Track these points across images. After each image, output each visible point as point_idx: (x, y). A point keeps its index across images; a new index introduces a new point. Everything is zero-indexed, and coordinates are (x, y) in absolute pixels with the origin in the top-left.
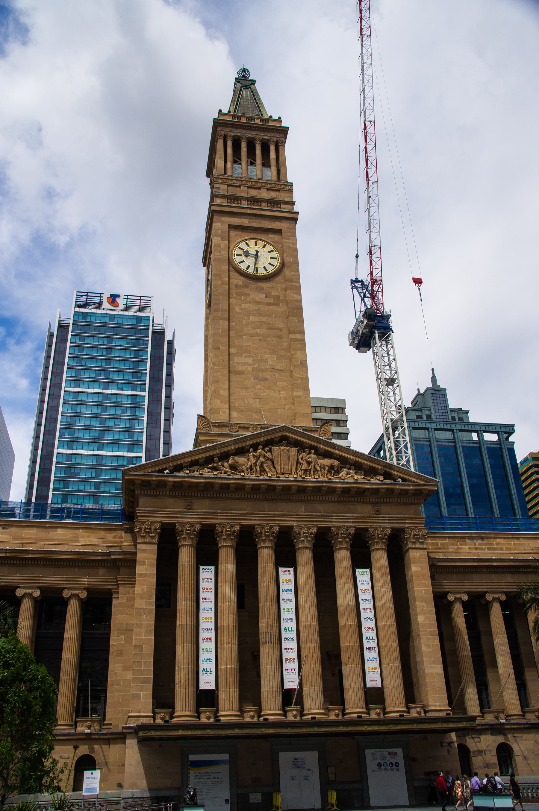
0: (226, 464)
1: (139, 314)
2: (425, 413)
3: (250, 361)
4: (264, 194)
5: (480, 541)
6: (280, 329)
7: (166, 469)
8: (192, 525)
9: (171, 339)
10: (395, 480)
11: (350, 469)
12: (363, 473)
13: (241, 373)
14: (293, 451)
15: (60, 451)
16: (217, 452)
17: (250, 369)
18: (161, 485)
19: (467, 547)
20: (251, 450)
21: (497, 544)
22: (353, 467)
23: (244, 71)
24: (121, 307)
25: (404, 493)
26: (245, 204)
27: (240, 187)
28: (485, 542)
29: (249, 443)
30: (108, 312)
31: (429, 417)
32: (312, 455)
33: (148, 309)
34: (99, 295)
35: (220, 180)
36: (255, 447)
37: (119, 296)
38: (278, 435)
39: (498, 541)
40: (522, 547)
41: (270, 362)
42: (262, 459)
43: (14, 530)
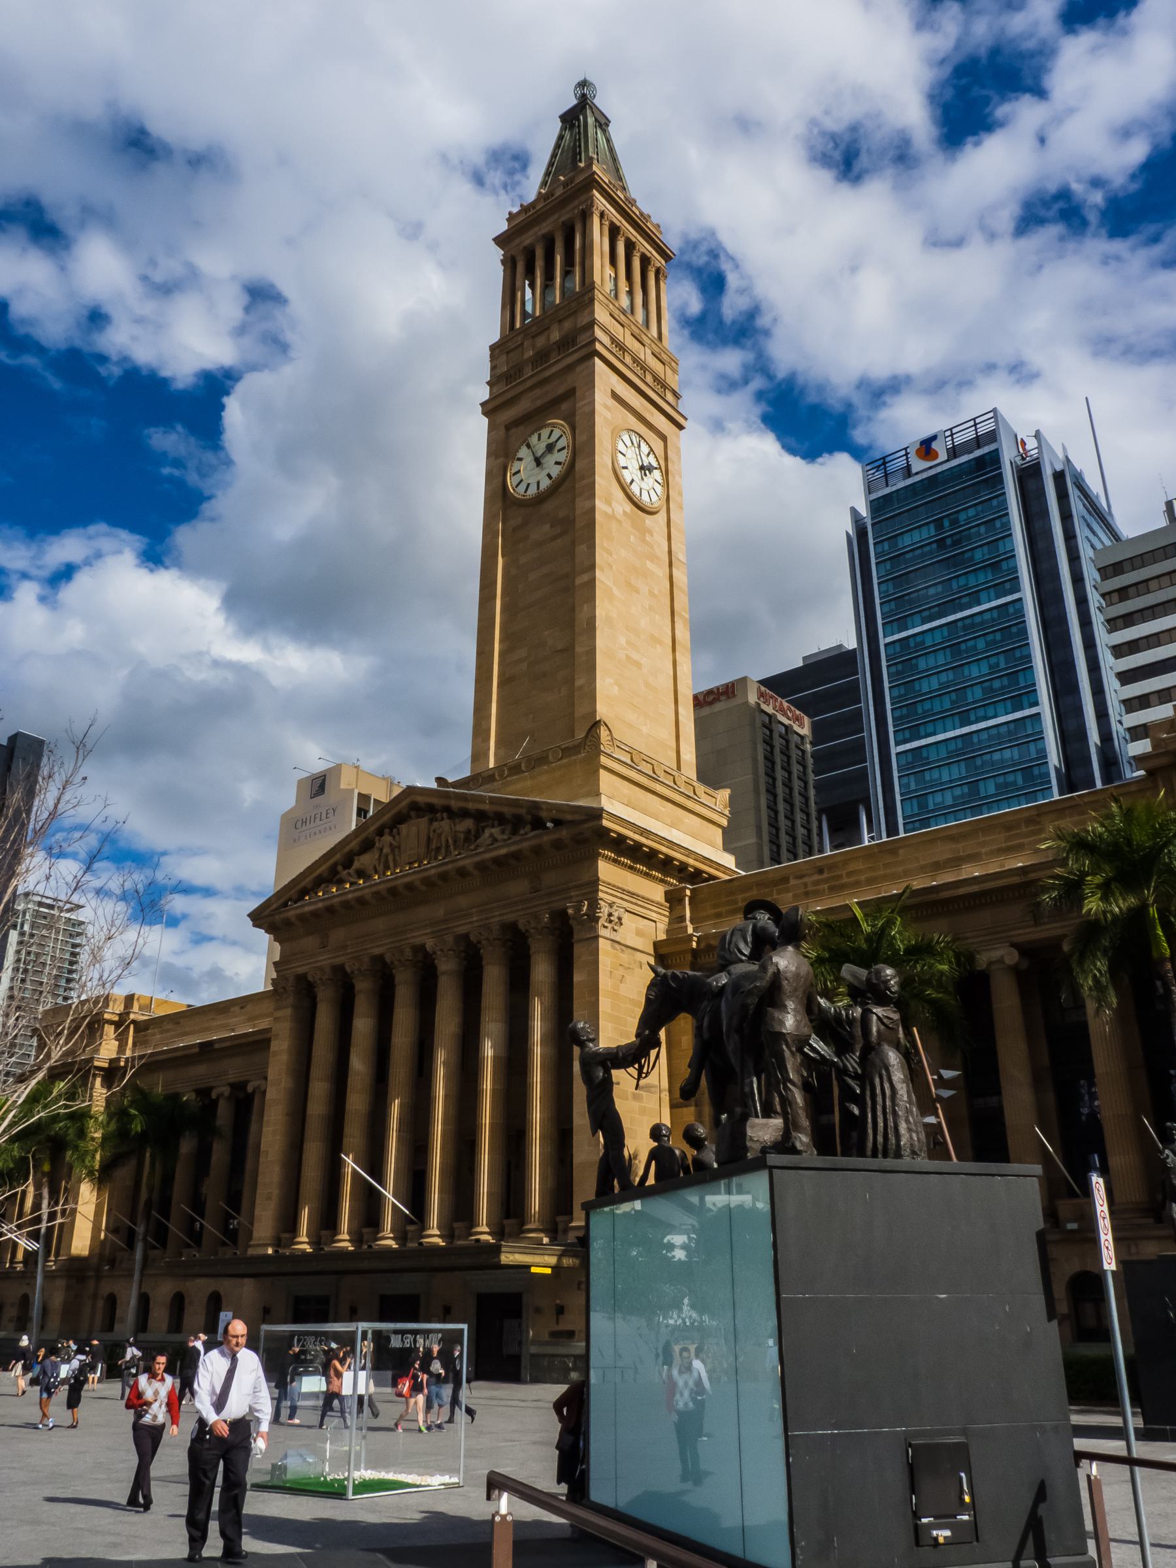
0: (352, 871)
3: (521, 653)
4: (555, 336)
5: (816, 877)
8: (321, 969)
9: (1059, 468)
11: (493, 826)
12: (509, 828)
14: (423, 822)
15: (901, 748)
16: (338, 857)
18: (288, 923)
19: (790, 895)
21: (849, 874)
22: (496, 823)
24: (943, 456)
25: (558, 845)
27: (522, 344)
28: (825, 875)
29: (372, 829)
30: (925, 475)
34: (903, 452)
36: (380, 833)
37: (934, 438)
38: (404, 803)
39: (852, 867)
40: (901, 869)
42: (386, 850)
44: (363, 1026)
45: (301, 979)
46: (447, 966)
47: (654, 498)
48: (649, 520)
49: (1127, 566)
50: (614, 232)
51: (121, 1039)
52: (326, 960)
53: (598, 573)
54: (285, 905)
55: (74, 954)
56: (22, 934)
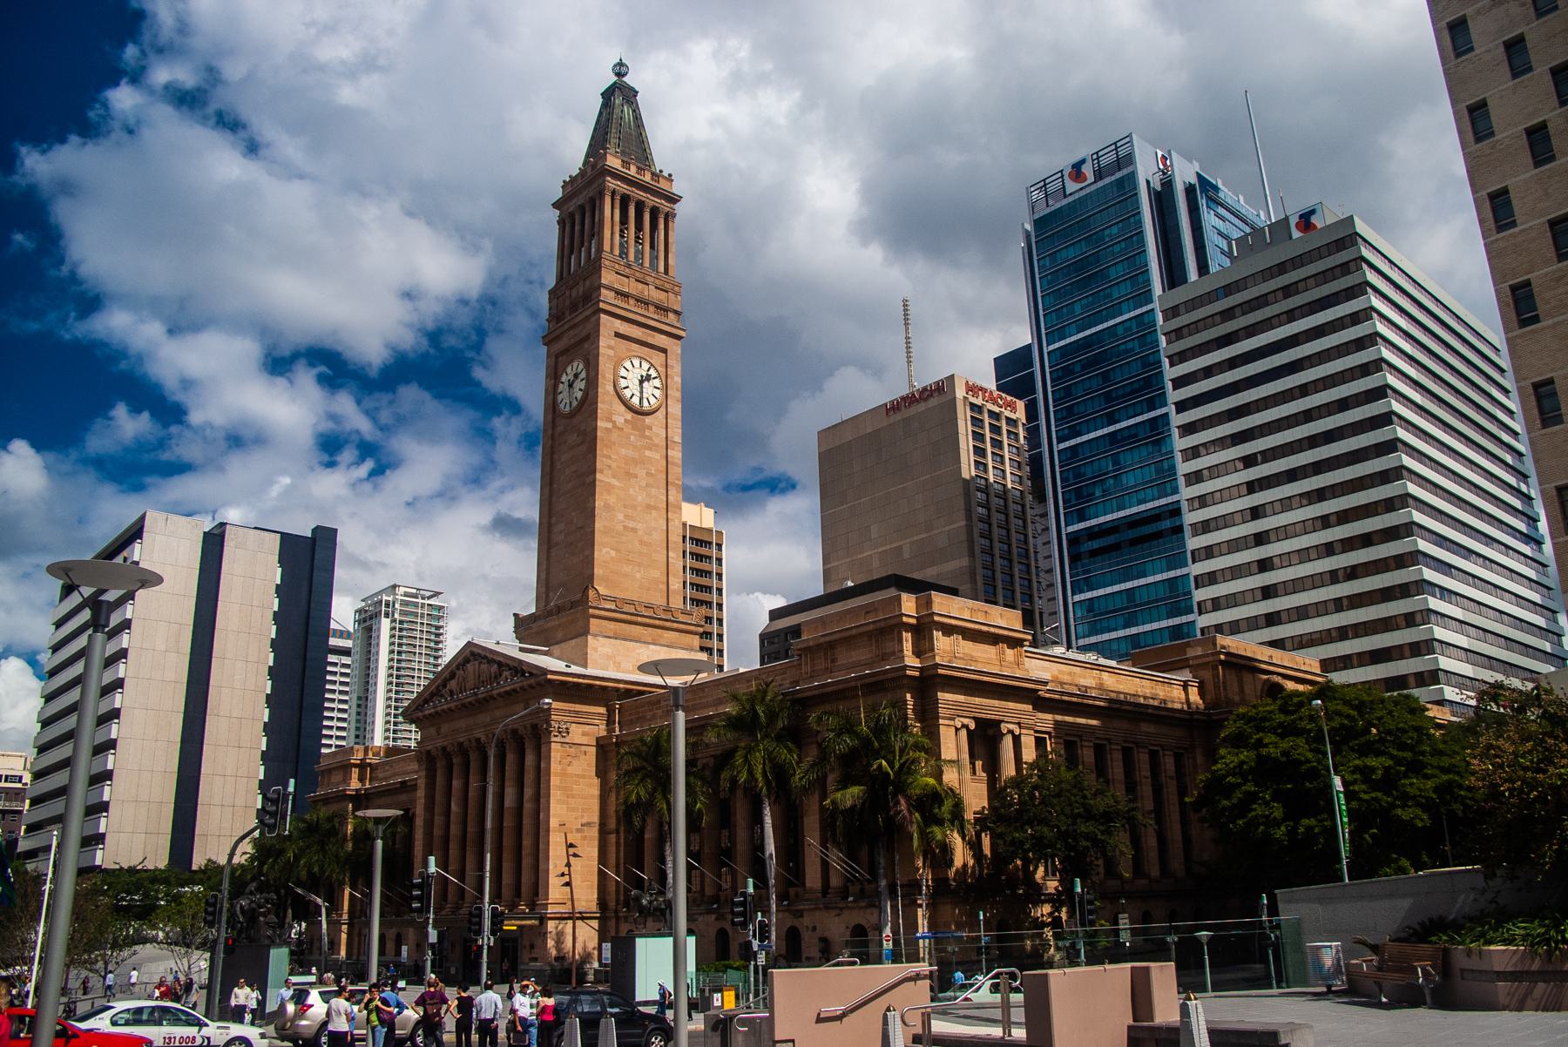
1: (1118, 175)
3: (561, 526)
23: (621, 64)
24: (1091, 179)
30: (1077, 196)
33: (1129, 159)
37: (1083, 161)
44: (457, 784)
45: (428, 752)
46: (492, 753)
47: (653, 401)
48: (648, 420)
49: (1182, 309)
50: (625, 200)
51: (361, 779)
52: (440, 743)
53: (598, 476)
55: (438, 635)
56: (394, 621)
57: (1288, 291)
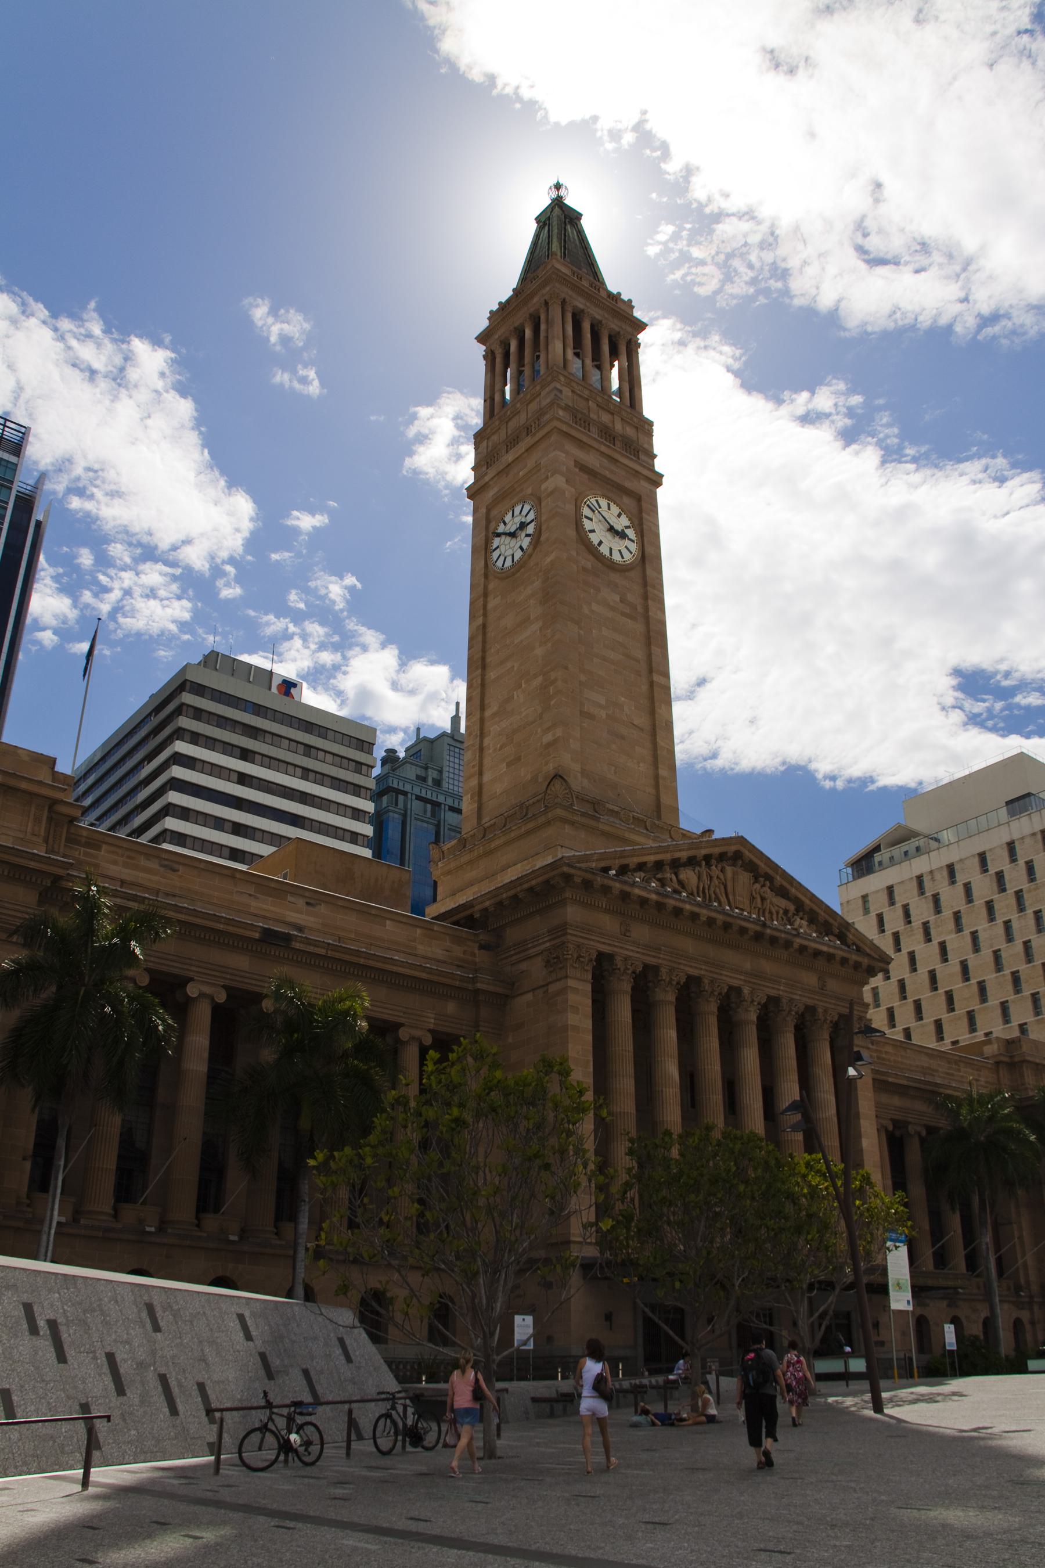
2: (432, 774)
6: (637, 660)
7: (609, 868)
9: (41, 518)
10: (849, 947)
11: (801, 919)
13: (591, 717)
17: (603, 714)
20: (704, 863)
23: (558, 186)
26: (594, 432)
27: (587, 400)
29: (704, 852)
31: (438, 783)
32: (766, 889)
35: (562, 379)
41: (626, 708)
43: (323, 909)
54: (606, 870)
57: (309, 750)
